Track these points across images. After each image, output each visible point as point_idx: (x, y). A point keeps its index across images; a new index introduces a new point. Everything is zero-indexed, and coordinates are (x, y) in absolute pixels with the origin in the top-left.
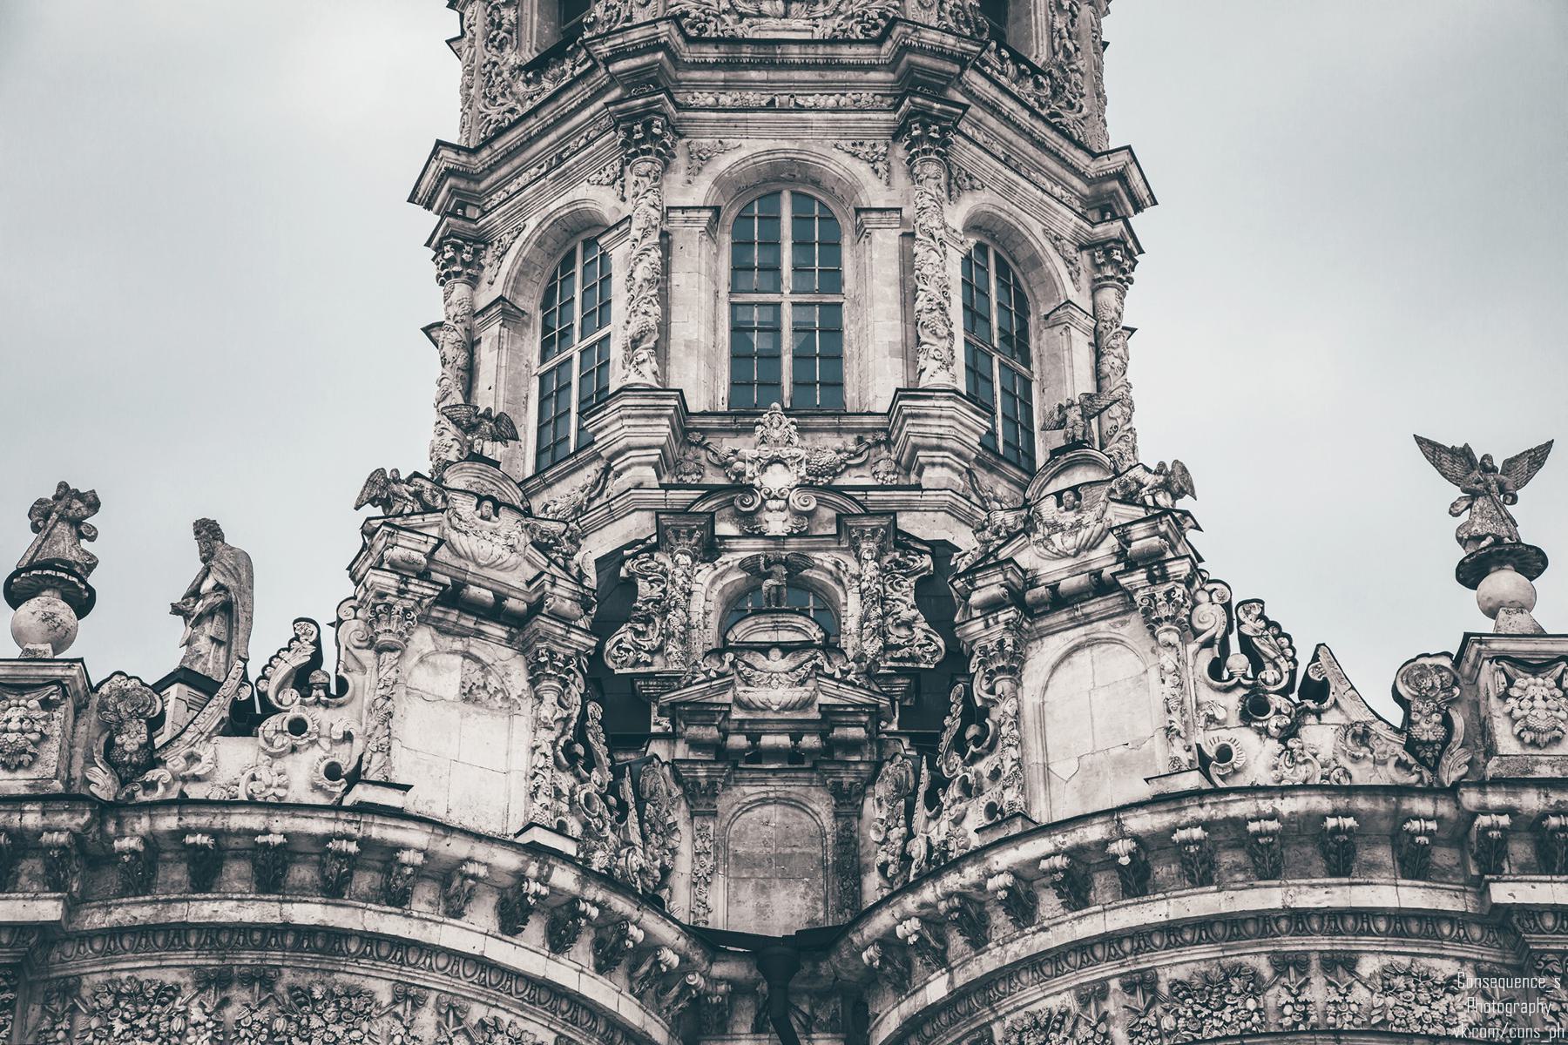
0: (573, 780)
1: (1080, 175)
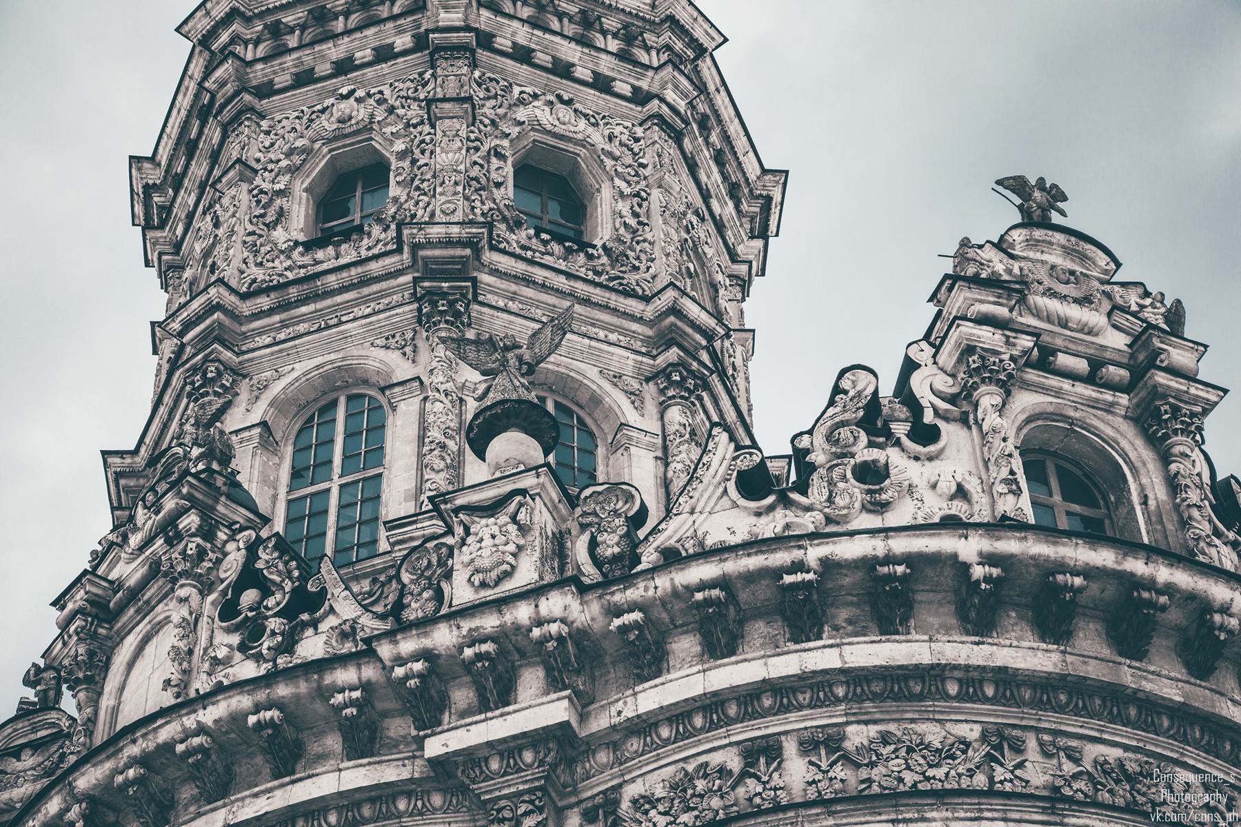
1: (640, 320)
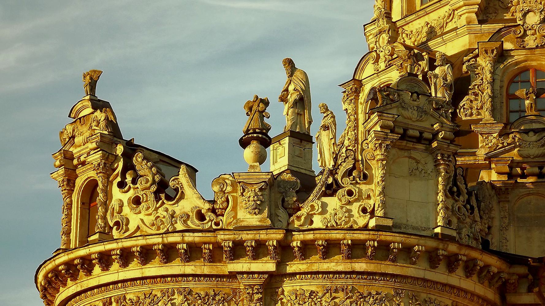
0: (453, 201)
